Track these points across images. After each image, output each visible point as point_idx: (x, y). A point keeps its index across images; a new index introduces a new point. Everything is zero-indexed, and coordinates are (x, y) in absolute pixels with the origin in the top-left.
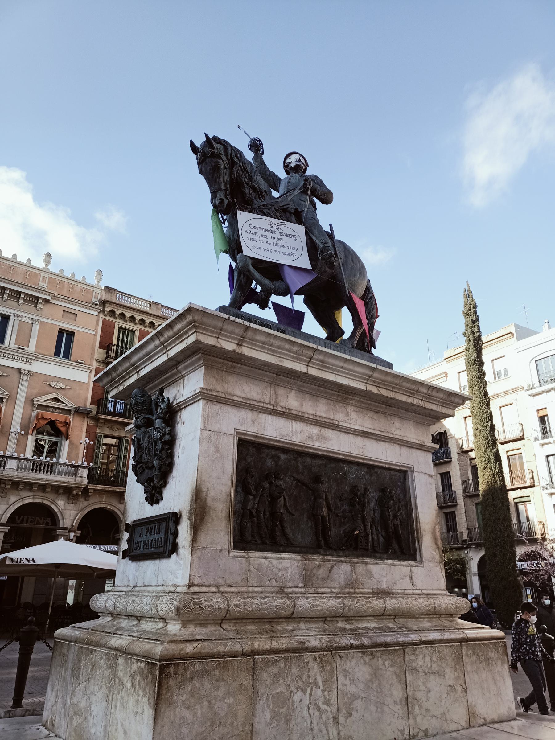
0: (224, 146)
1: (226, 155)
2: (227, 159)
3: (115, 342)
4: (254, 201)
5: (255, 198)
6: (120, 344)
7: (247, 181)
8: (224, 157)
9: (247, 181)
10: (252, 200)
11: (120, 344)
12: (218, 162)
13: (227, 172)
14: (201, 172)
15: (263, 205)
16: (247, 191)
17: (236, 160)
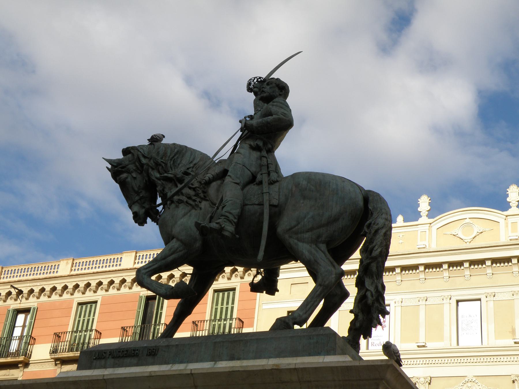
2: (136, 166)
8: (132, 167)
9: (158, 175)
17: (144, 161)
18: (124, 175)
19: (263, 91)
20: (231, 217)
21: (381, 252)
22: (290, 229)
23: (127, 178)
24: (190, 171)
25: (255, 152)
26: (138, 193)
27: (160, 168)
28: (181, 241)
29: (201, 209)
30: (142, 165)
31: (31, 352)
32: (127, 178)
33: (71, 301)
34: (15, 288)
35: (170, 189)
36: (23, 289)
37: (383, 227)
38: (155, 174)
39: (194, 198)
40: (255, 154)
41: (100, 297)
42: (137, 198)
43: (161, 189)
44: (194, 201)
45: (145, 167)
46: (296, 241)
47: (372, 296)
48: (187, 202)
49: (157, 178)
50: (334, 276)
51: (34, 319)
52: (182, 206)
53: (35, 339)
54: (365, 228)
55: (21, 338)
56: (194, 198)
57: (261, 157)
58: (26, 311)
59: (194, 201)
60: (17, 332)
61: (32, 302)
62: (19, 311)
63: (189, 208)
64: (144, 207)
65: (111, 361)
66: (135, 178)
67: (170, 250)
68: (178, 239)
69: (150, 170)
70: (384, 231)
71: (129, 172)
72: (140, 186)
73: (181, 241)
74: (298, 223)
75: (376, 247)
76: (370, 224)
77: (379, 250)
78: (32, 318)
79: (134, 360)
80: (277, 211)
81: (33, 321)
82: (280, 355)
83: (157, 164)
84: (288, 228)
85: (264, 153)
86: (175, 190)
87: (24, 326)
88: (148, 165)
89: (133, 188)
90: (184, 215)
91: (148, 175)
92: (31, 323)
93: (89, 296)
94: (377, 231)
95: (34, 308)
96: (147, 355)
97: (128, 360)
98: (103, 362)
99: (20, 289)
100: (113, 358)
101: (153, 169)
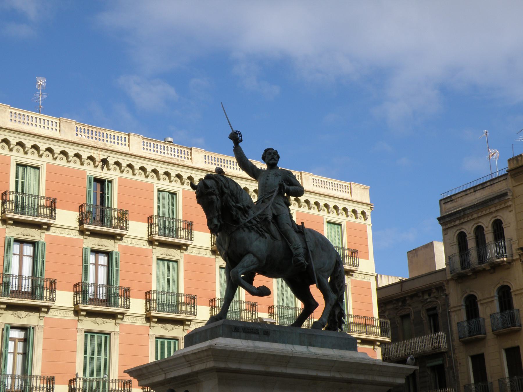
0: (216, 181)
1: (218, 189)
2: (219, 191)
3: (12, 188)
4: (241, 219)
5: (241, 216)
6: (20, 190)
7: (234, 204)
9: (234, 204)
10: (238, 219)
11: (20, 190)
12: (212, 198)
13: (219, 201)
14: (199, 202)
15: (248, 222)
16: (234, 213)
17: (226, 190)
19: (273, 158)
24: (250, 205)
26: (218, 212)
27: (234, 198)
28: (258, 258)
29: (266, 238)
39: (261, 229)
44: (261, 231)
45: (226, 195)
49: (233, 205)
56: (261, 229)
59: (261, 231)
63: (258, 235)
64: (220, 222)
65: (243, 335)
66: (218, 200)
67: (252, 262)
68: (255, 256)
69: (229, 198)
71: (216, 195)
73: (258, 258)
79: (257, 336)
82: (333, 347)
88: (228, 194)
90: (256, 239)
96: (264, 334)
97: (253, 335)
98: (238, 334)
101: (231, 198)
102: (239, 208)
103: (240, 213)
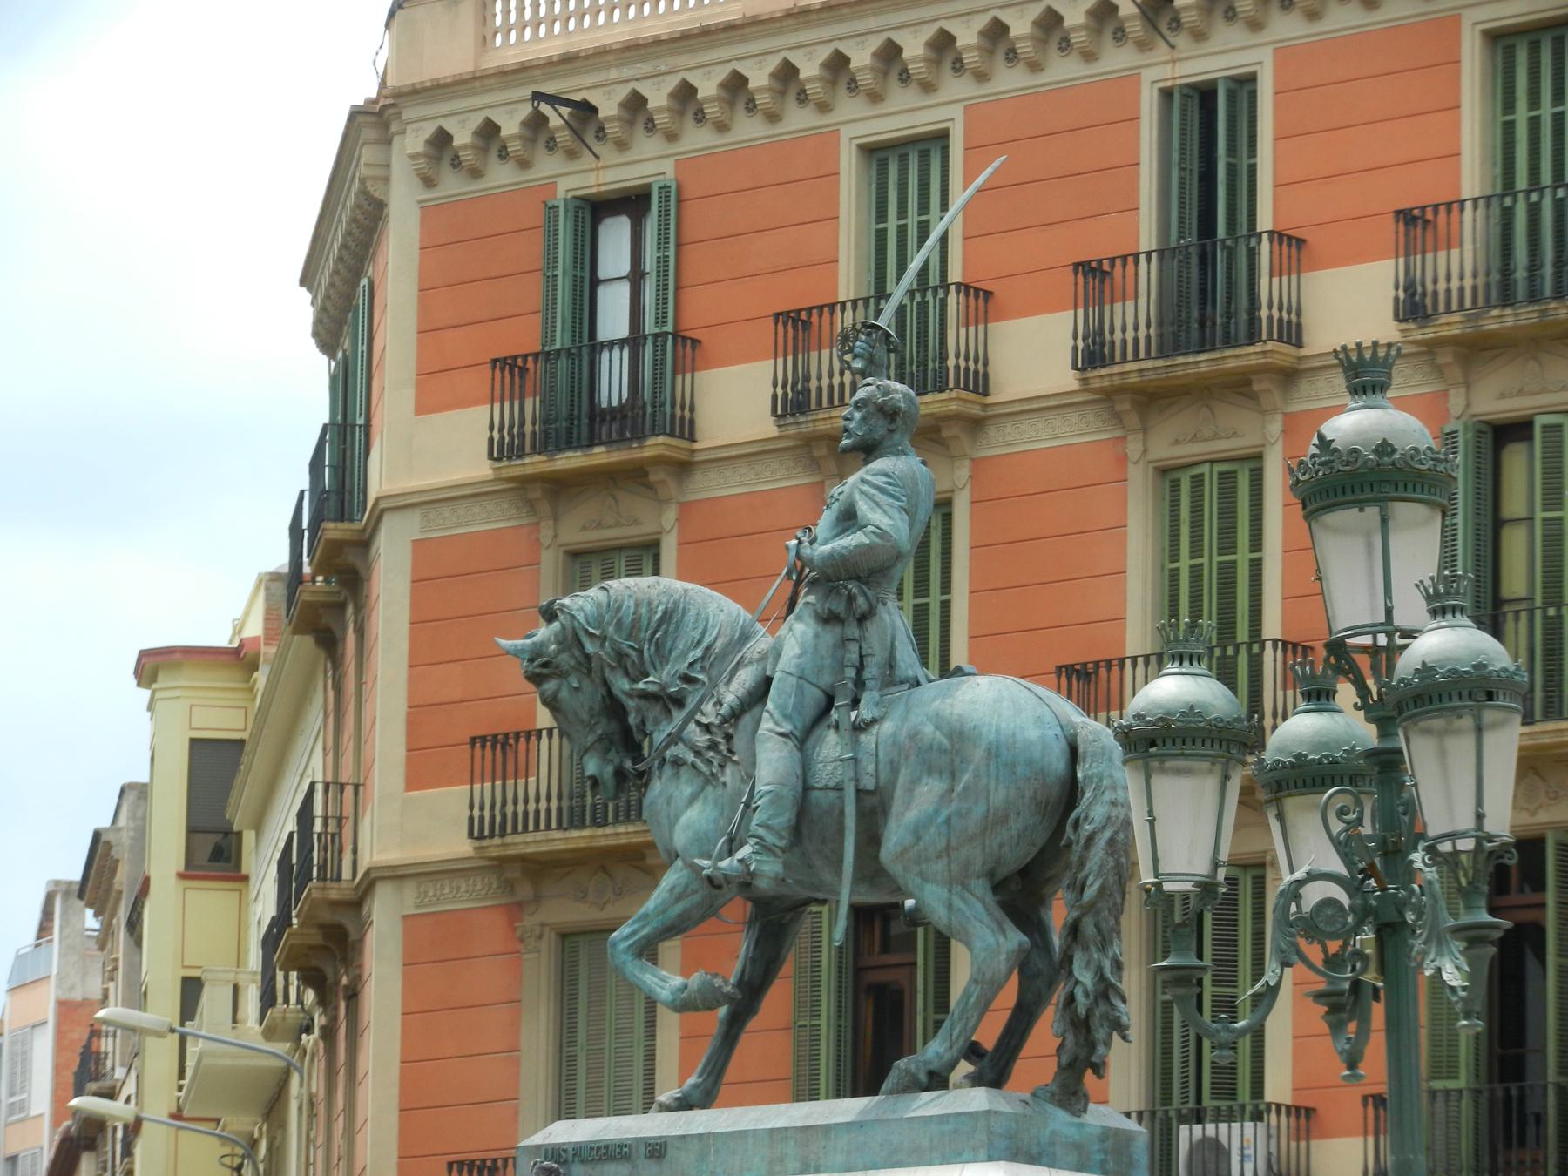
8: (565, 660)
17: (590, 648)
18: (550, 686)
20: (771, 839)
21: (1102, 889)
22: (902, 854)
23: (558, 691)
25: (828, 628)
29: (724, 784)
30: (588, 657)
31: (692, 410)
32: (558, 691)
33: (829, 138)
34: (554, 100)
35: (657, 723)
36: (594, 98)
37: (1104, 827)
38: (621, 684)
40: (830, 636)
41: (957, 112)
42: (591, 739)
43: (638, 721)
46: (918, 880)
47: (1087, 994)
48: (694, 766)
49: (625, 693)
50: (1003, 957)
51: (677, 240)
52: (685, 773)
53: (696, 342)
54: (1069, 829)
55: (635, 341)
57: (845, 641)
58: (633, 203)
59: (709, 762)
60: (613, 319)
61: (645, 163)
62: (597, 209)
70: (1107, 834)
72: (591, 709)
74: (919, 839)
75: (1091, 878)
76: (1077, 821)
77: (1097, 885)
78: (662, 243)
80: (874, 809)
81: (671, 253)
83: (620, 656)
84: (899, 849)
85: (853, 630)
86: (669, 728)
87: (636, 277)
89: (575, 713)
90: (693, 799)
91: (605, 683)
92: (662, 263)
93: (905, 114)
94: (1090, 839)
95: (665, 189)
99: (577, 97)
100: (582, 1162)
101: (612, 668)
102: (645, 696)
103: (654, 711)
